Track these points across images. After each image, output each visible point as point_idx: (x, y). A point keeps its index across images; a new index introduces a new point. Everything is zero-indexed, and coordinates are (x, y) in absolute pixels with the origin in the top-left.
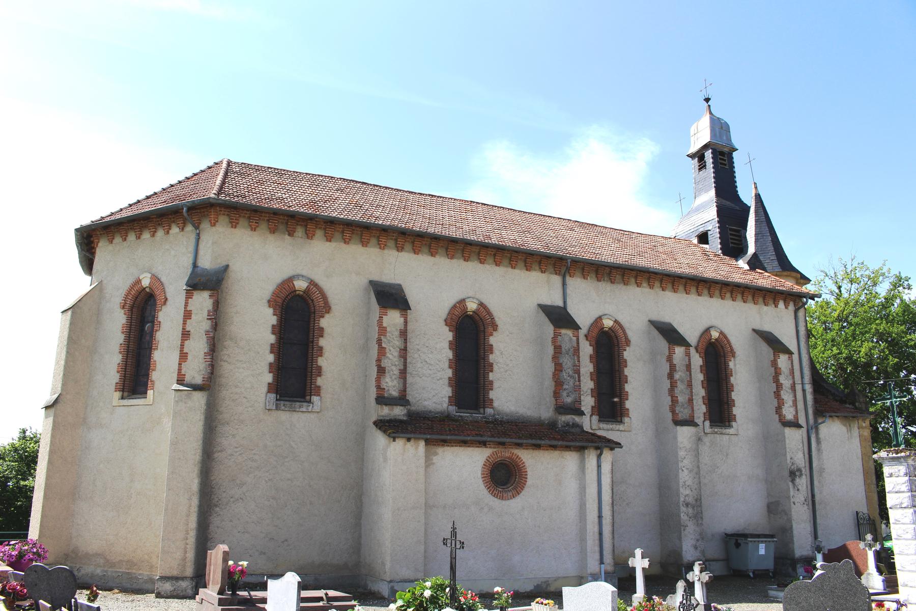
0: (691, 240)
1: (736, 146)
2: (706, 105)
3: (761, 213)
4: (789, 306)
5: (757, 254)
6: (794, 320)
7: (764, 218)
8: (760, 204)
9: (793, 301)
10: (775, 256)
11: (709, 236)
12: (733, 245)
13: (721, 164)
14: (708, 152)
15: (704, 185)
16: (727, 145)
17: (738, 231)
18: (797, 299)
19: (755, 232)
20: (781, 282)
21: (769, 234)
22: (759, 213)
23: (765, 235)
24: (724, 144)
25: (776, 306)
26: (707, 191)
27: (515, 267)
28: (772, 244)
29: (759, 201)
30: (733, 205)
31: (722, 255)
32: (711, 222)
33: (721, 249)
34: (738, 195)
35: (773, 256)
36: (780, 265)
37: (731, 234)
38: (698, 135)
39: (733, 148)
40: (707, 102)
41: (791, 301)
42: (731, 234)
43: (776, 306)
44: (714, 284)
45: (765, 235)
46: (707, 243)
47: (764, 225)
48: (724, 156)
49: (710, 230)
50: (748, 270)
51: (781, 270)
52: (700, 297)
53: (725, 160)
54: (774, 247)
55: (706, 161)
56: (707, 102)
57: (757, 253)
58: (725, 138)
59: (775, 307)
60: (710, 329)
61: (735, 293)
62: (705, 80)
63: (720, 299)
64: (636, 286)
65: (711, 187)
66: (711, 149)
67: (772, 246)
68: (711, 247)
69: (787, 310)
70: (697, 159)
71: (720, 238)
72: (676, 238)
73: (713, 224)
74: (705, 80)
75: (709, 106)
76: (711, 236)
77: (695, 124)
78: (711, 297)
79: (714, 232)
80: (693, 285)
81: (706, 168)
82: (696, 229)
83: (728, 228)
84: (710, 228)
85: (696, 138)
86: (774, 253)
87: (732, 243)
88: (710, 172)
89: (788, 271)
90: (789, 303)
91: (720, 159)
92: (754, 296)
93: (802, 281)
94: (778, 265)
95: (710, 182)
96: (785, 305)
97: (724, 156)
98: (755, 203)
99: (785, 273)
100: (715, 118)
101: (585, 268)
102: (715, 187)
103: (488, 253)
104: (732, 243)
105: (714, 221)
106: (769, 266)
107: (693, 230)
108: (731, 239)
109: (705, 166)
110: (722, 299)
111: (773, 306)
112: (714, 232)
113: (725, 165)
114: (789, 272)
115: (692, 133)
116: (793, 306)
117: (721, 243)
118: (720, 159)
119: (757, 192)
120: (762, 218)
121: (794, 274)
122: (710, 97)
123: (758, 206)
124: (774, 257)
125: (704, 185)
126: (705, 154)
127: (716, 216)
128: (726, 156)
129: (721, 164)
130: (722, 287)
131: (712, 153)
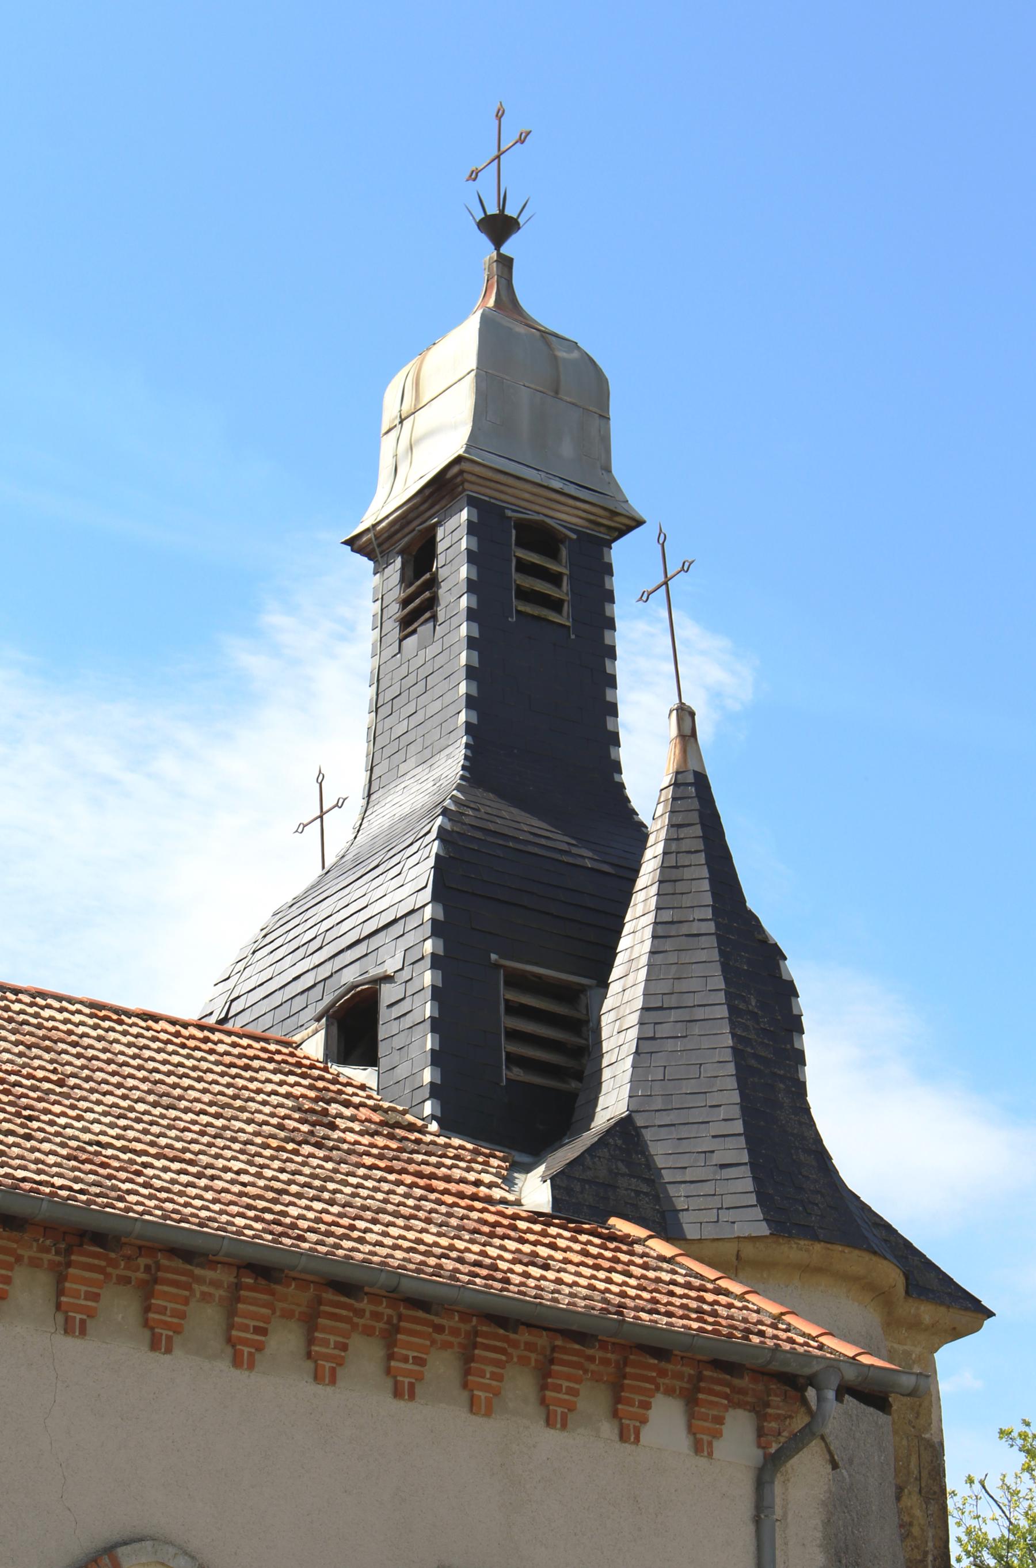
0: (297, 1038)
1: (637, 502)
2: (487, 251)
3: (695, 886)
4: (717, 1435)
5: (637, 1129)
6: (751, 1528)
7: (708, 913)
8: (698, 831)
9: (753, 1409)
10: (742, 1142)
11: (384, 1014)
12: (518, 1074)
13: (524, 595)
14: (451, 524)
15: (419, 717)
16: (572, 490)
17: (570, 995)
18: (775, 1399)
19: (646, 994)
20: (727, 1293)
21: (723, 1012)
22: (680, 887)
23: (700, 1013)
24: (557, 485)
25: (628, 1435)
26: (428, 756)
27: (333, 1372)
28: (731, 1069)
29: (695, 817)
30: (561, 840)
31: (434, 1127)
32: (397, 929)
33: (435, 1091)
34: (622, 786)
35: (731, 1143)
36: (763, 1199)
37: (513, 1009)
38: (422, 421)
39: (633, 519)
40: (498, 241)
41: (739, 1405)
42: (513, 1009)
43: (628, 1435)
44: (178, 1263)
45: (700, 1013)
46: (370, 1059)
47: (703, 956)
48: (553, 554)
49: (388, 979)
50: (535, 1217)
51: (764, 1229)
52: (71, 1344)
53: (555, 579)
54: (742, 1088)
55: (442, 574)
56: (498, 241)
57: (640, 1121)
58: (567, 449)
59: (623, 1437)
60: (121, 1551)
61: (332, 1331)
62: (500, 115)
63: (224, 1365)
64: (542, 1423)
65: (448, 726)
66: (472, 502)
67: (732, 1084)
68: (389, 1079)
69: (702, 1461)
70: (399, 561)
71: (436, 1025)
72: (229, 1026)
73: (410, 939)
74: (500, 115)
75: (505, 264)
76: (396, 1011)
77: (410, 367)
78: (155, 1345)
79: (412, 988)
80: (35, 1263)
81: (434, 618)
82: (324, 972)
83: (497, 966)
84: (390, 967)
85: (404, 442)
86: (738, 1127)
87: (513, 1060)
88: (448, 640)
89: (815, 1238)
90: (719, 1420)
91: (524, 567)
92: (622, 1388)
93: (927, 1312)
94: (753, 1199)
95: (448, 698)
96: (691, 1429)
97: (553, 554)
98: (671, 825)
99: (796, 1251)
100: (521, 329)
101: (322, 1321)
102: (469, 728)
103: (108, 1276)
104: (513, 1060)
105: (413, 921)
106: (700, 1202)
107: (308, 981)
108: (513, 1035)
109: (432, 603)
110: (237, 1362)
111: (608, 1429)
112: (412, 988)
113: (556, 605)
114: (818, 1247)
115: (391, 409)
116: (750, 1436)
117: (437, 1058)
118: (524, 567)
119: (692, 766)
120: (699, 914)
121: (855, 1261)
122: (511, 211)
123: (685, 845)
124: (737, 1151)
125: (419, 717)
126: (440, 533)
127: (427, 895)
128: (564, 553)
129: (524, 595)
130: (238, 1286)
131: (472, 529)
